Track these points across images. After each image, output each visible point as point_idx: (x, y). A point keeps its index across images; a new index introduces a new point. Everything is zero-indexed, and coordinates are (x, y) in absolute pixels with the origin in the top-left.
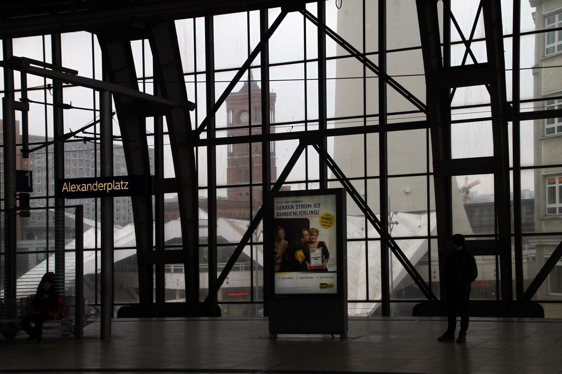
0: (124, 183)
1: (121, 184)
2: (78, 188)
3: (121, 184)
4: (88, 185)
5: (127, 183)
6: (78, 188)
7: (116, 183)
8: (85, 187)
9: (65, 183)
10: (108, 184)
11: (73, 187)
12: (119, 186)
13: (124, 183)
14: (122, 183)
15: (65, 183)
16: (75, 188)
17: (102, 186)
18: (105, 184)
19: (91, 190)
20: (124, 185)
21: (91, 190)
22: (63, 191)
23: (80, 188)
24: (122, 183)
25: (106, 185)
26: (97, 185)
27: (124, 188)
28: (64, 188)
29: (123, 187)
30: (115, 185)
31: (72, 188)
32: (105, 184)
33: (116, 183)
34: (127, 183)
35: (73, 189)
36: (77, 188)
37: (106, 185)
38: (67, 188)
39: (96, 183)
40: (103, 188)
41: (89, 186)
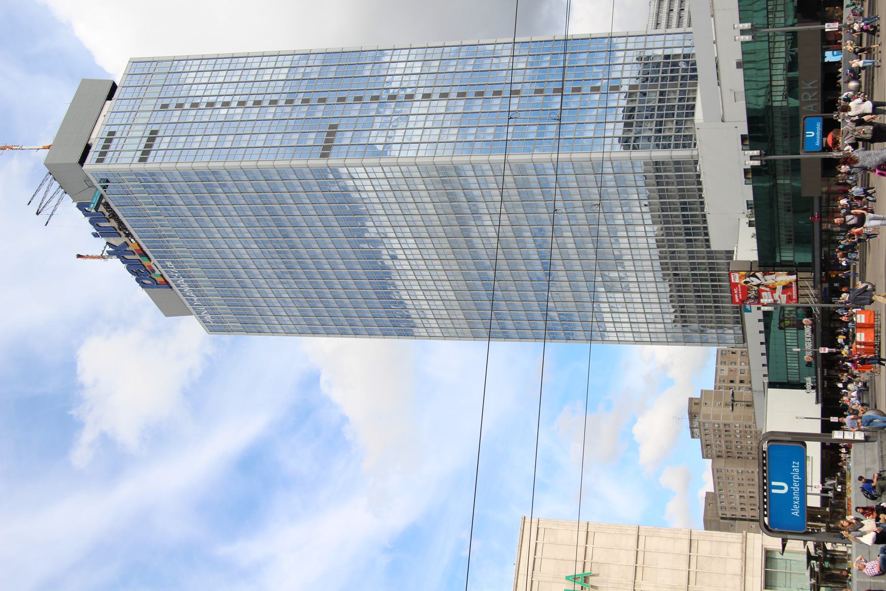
1: (795, 468)
3: (795, 468)
4: (794, 495)
5: (794, 462)
6: (796, 503)
8: (796, 497)
9: (793, 513)
12: (796, 469)
14: (793, 467)
15: (793, 513)
20: (795, 465)
23: (796, 501)
25: (795, 480)
28: (797, 515)
29: (797, 465)
31: (796, 508)
32: (794, 481)
33: (794, 471)
34: (794, 462)
36: (796, 504)
37: (795, 480)
38: (797, 513)
41: (795, 494)
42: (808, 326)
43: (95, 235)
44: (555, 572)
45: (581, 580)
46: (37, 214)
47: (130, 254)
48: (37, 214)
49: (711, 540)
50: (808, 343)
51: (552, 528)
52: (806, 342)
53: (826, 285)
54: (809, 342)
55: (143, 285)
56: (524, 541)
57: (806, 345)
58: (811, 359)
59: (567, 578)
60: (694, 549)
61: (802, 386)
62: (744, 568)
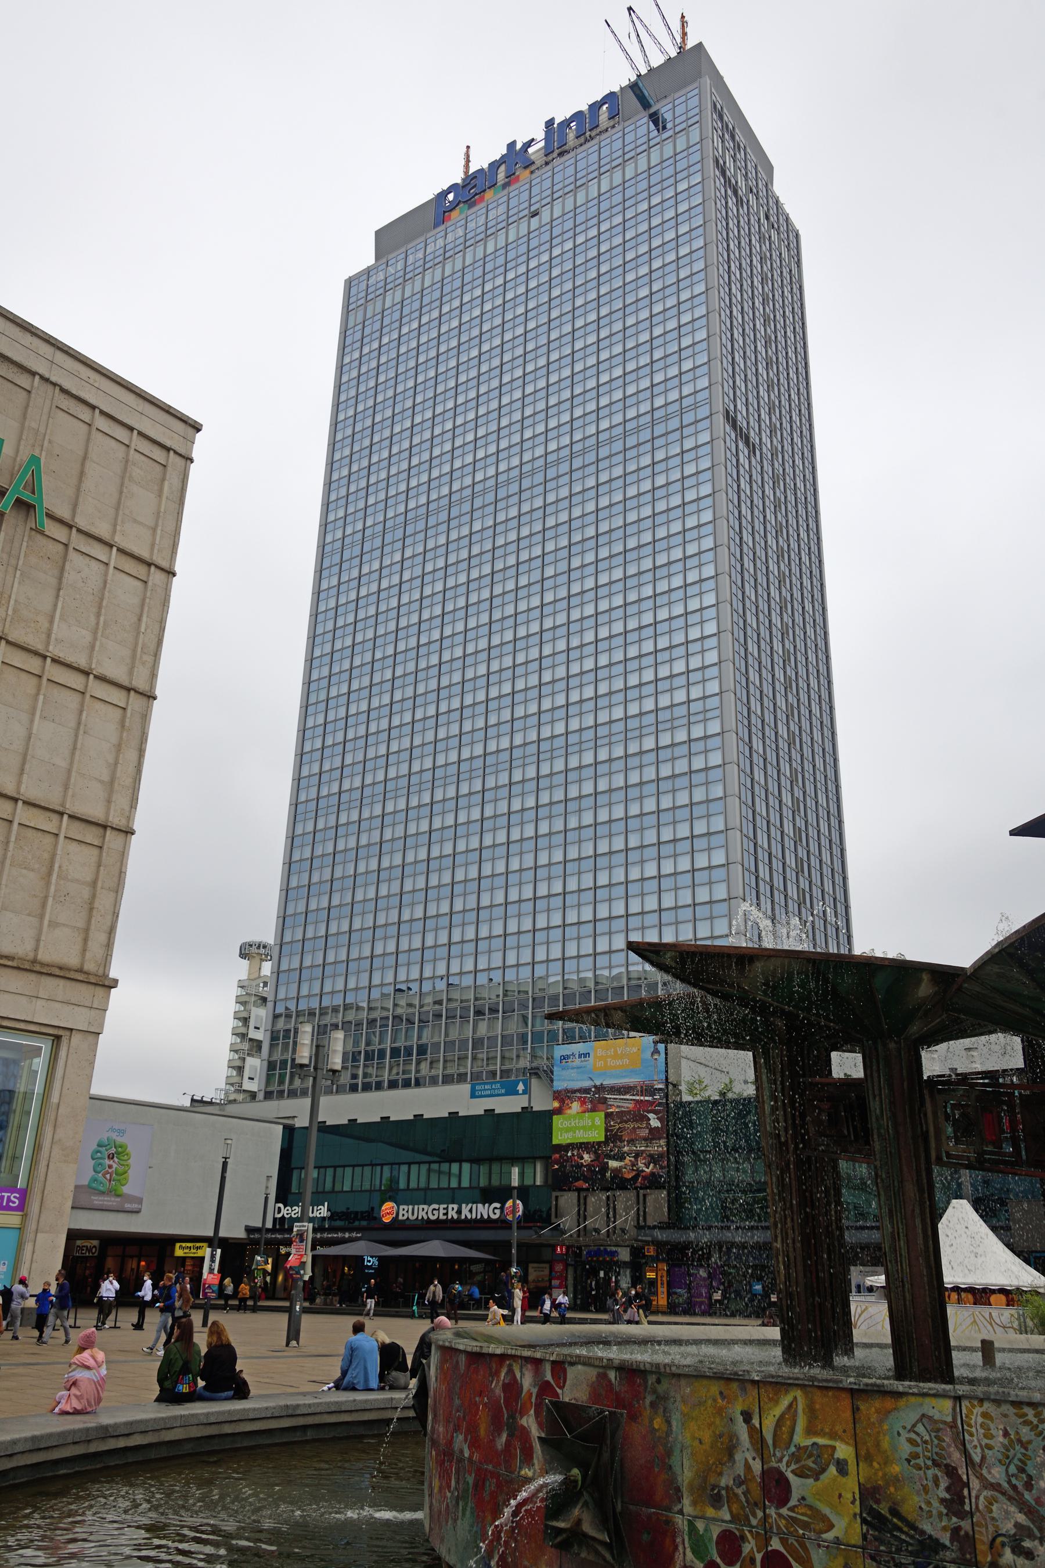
42: (498, 1212)
43: (550, 123)
44: (50, 442)
45: (26, 496)
46: (630, 9)
47: (507, 170)
48: (630, 9)
49: (99, 884)
50: (442, 1211)
51: (166, 483)
52: (442, 1206)
53: (624, 1255)
54: (446, 1214)
55: (443, 194)
56: (141, 401)
57: (436, 1206)
58: (387, 1220)
59: (35, 460)
60: (77, 830)
61: (284, 1195)
62: (10, 963)
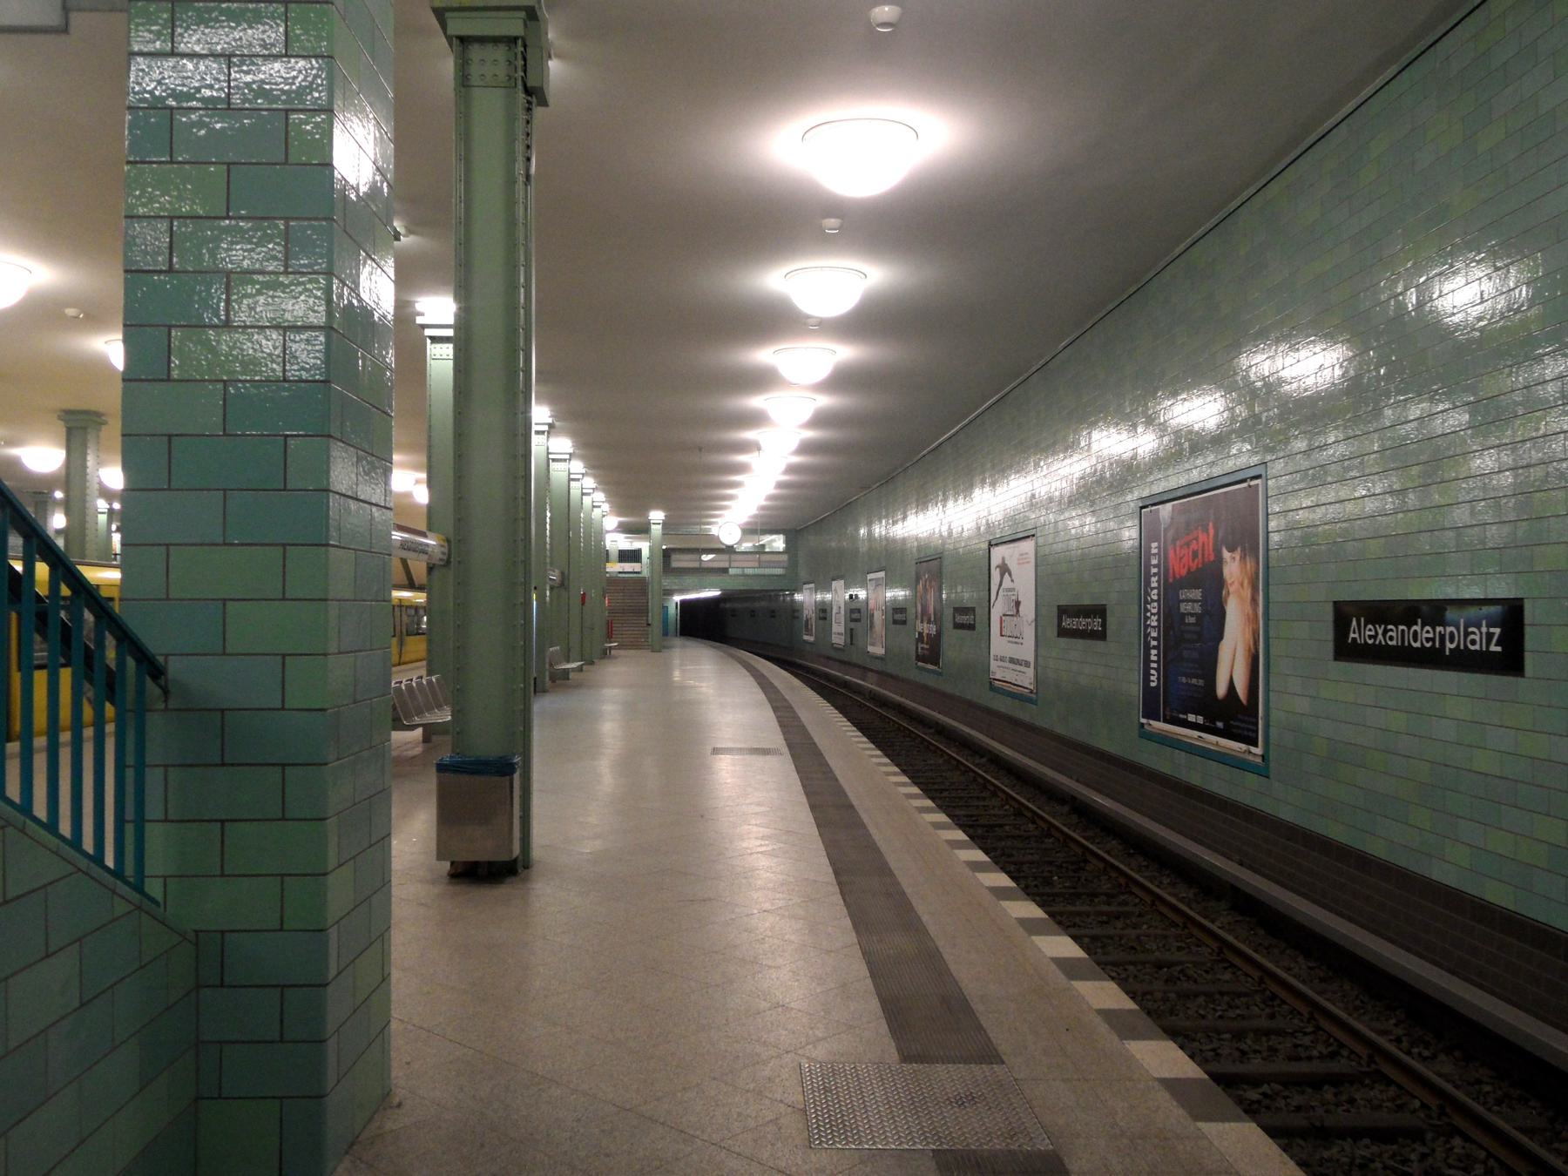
0: (1492, 630)
1: (1481, 633)
2: (1380, 637)
3: (1481, 633)
5: (1497, 631)
7: (1471, 630)
10: (1449, 629)
11: (1370, 630)
13: (1492, 630)
16: (1373, 633)
17: (1431, 635)
18: (1439, 629)
19: (1406, 644)
20: (1490, 636)
21: (1406, 644)
22: (1350, 641)
24: (1484, 629)
25: (1442, 637)
26: (1419, 630)
27: (1494, 648)
28: (1352, 635)
30: (1467, 634)
34: (1497, 631)
35: (1370, 637)
38: (1356, 636)
39: (1416, 624)
40: (1433, 640)
41: (1403, 631)
